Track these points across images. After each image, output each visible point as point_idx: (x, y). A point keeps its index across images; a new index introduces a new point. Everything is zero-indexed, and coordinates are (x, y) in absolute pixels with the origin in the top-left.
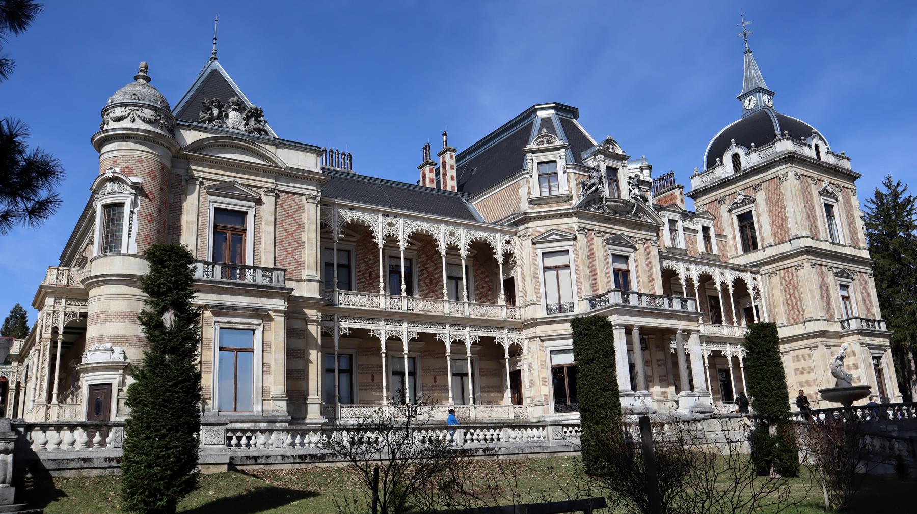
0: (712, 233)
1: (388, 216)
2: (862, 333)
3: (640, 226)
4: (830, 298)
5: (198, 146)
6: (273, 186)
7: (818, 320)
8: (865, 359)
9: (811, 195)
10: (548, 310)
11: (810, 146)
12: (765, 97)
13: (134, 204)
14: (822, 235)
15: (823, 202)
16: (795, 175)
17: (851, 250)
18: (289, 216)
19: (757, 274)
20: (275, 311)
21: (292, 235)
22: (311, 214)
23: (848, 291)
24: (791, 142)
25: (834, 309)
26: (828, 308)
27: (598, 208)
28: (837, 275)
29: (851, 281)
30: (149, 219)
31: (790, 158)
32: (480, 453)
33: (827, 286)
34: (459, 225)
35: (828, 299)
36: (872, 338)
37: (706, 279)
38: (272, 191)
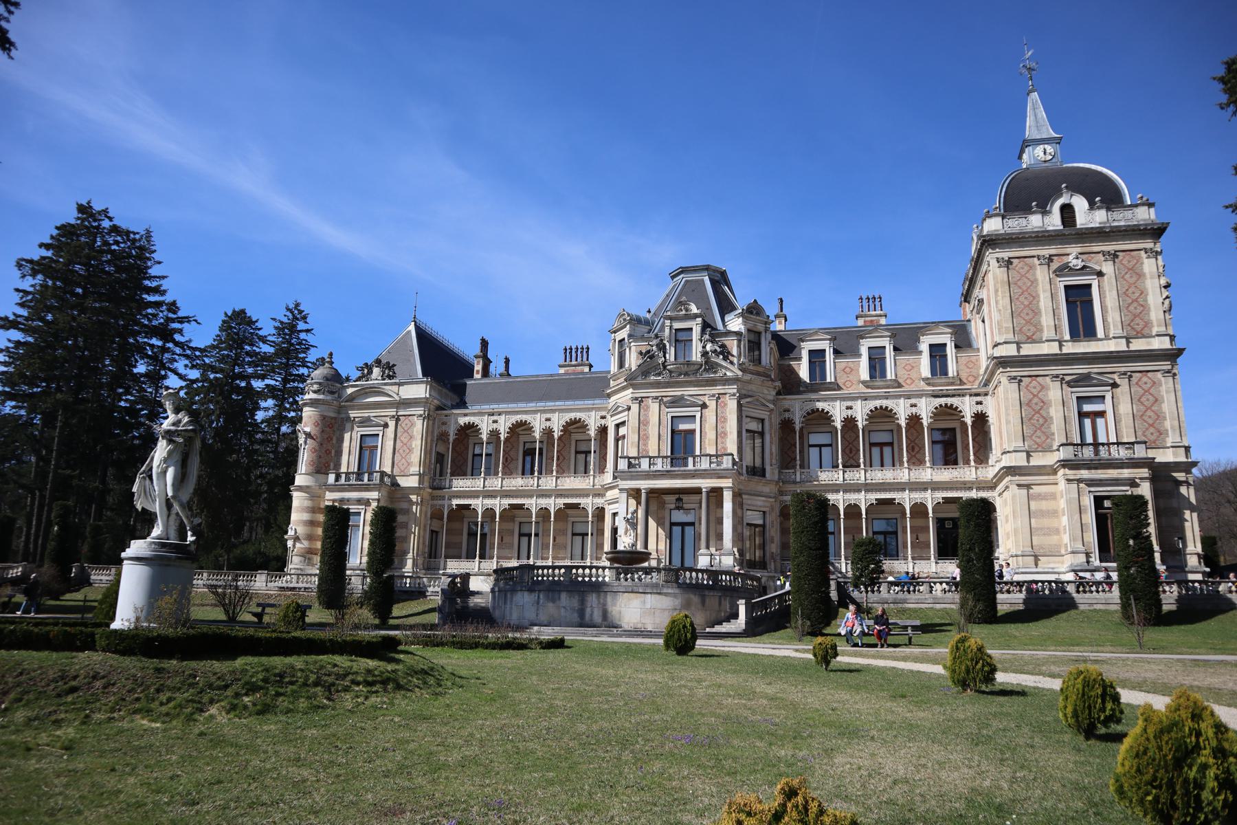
0: (950, 351)
1: (493, 415)
2: (1066, 464)
3: (712, 383)
4: (1047, 420)
5: (352, 398)
6: (394, 413)
7: (1009, 452)
8: (1069, 502)
9: (1034, 282)
10: (615, 478)
11: (1045, 212)
12: (1039, 151)
13: (305, 442)
14: (1048, 333)
15: (1062, 286)
16: (998, 262)
17: (1117, 344)
18: (406, 431)
19: (986, 394)
20: (372, 499)
21: (406, 444)
22: (418, 427)
23: (1104, 403)
24: (1000, 219)
25: (1053, 434)
26: (1039, 434)
27: (659, 374)
28: (1069, 384)
29: (1109, 388)
30: (314, 451)
31: (989, 242)
32: (303, 590)
33: (1045, 404)
34: (553, 411)
35: (1041, 421)
36: (1099, 471)
37: (882, 416)
38: (393, 417)
